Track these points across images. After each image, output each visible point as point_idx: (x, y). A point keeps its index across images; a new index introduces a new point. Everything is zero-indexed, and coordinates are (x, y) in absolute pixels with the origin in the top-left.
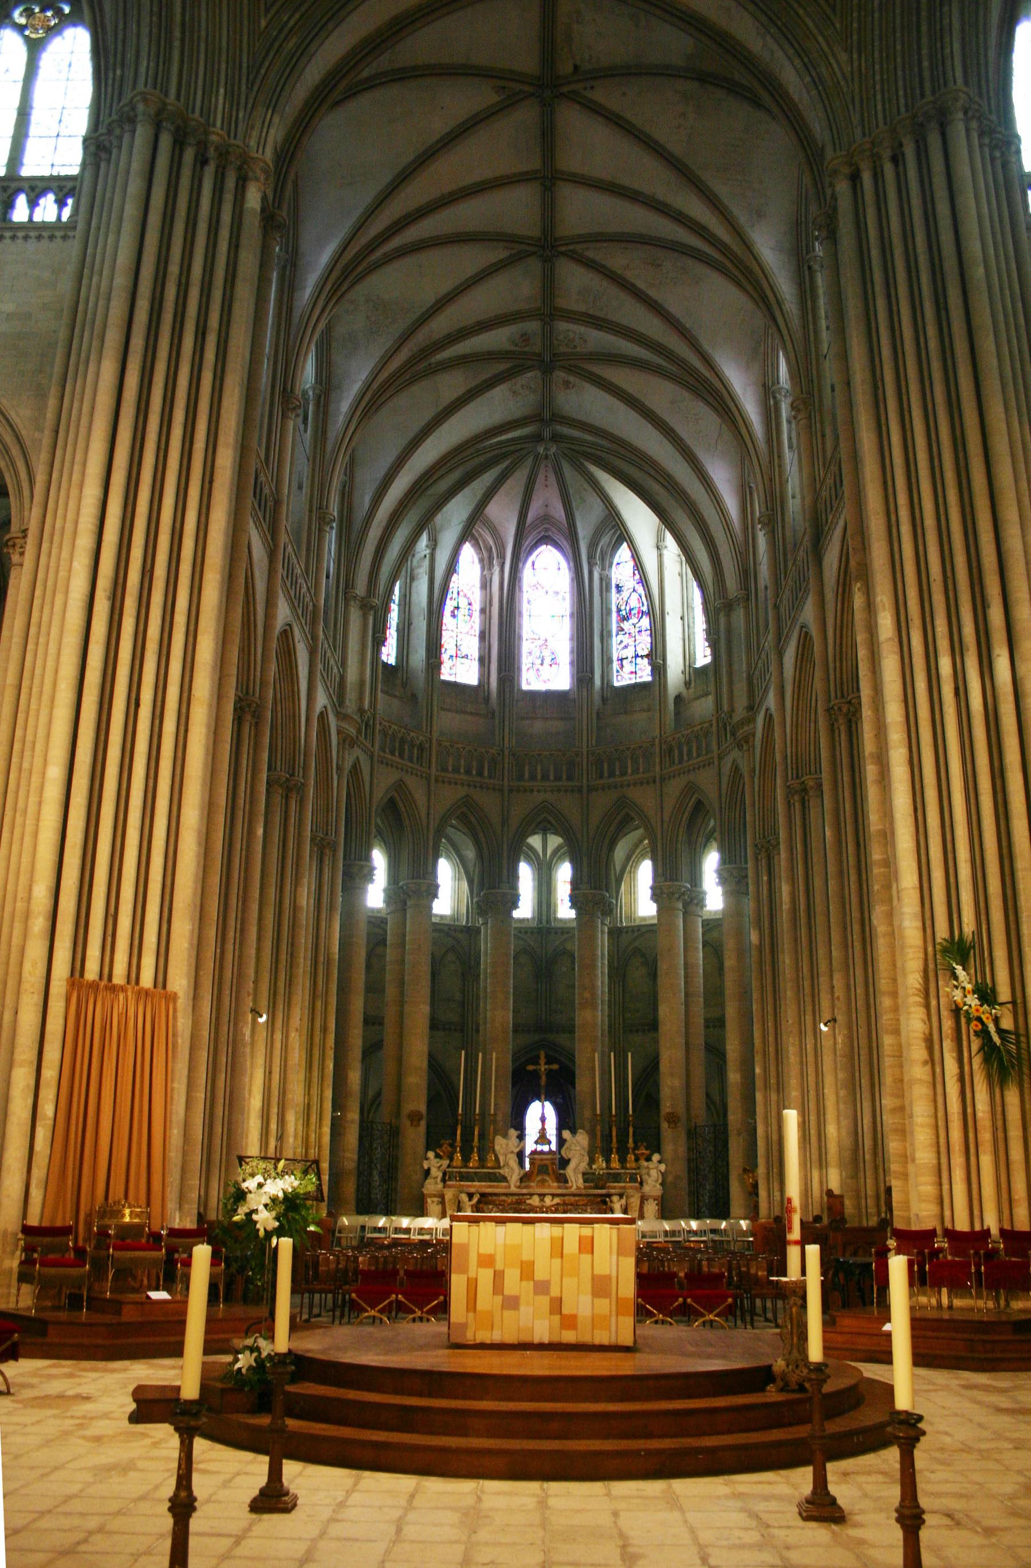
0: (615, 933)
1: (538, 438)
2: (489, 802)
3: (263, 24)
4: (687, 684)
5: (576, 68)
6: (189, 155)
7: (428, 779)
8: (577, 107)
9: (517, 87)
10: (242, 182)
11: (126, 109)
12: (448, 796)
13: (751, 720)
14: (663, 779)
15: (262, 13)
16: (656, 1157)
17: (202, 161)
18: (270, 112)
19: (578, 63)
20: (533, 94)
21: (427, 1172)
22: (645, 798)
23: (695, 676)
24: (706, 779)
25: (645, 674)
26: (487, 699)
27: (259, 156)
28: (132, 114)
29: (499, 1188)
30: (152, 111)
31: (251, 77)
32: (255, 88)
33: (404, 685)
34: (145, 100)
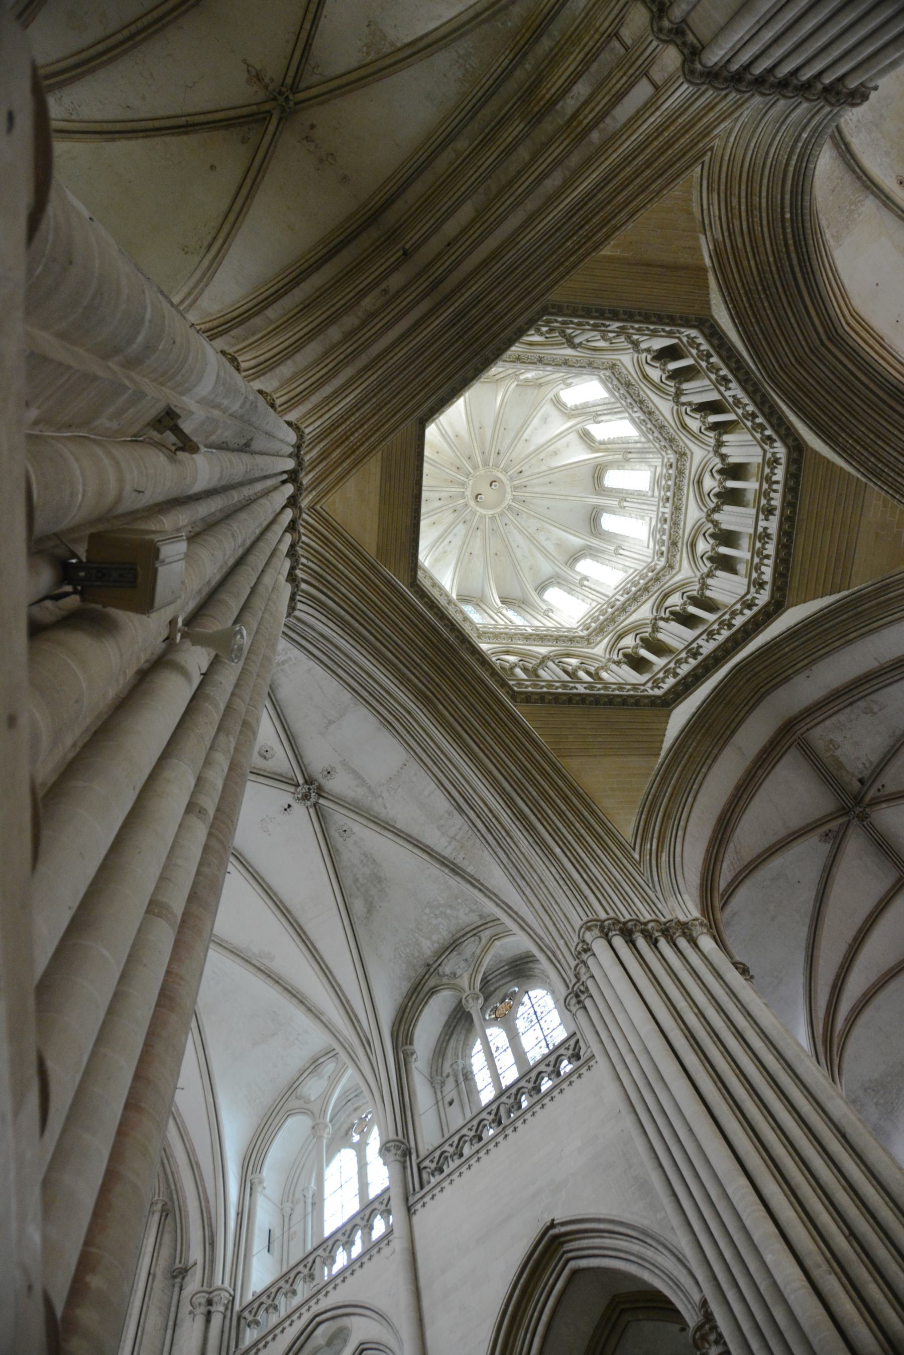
3: (637, 856)
5: (861, 781)
6: (641, 942)
8: (884, 805)
9: (834, 825)
11: (580, 945)
15: (632, 851)
17: (654, 943)
18: (678, 896)
19: (860, 776)
20: (849, 821)
27: (690, 918)
28: (585, 947)
30: (596, 932)
31: (651, 885)
32: (658, 888)
34: (589, 929)
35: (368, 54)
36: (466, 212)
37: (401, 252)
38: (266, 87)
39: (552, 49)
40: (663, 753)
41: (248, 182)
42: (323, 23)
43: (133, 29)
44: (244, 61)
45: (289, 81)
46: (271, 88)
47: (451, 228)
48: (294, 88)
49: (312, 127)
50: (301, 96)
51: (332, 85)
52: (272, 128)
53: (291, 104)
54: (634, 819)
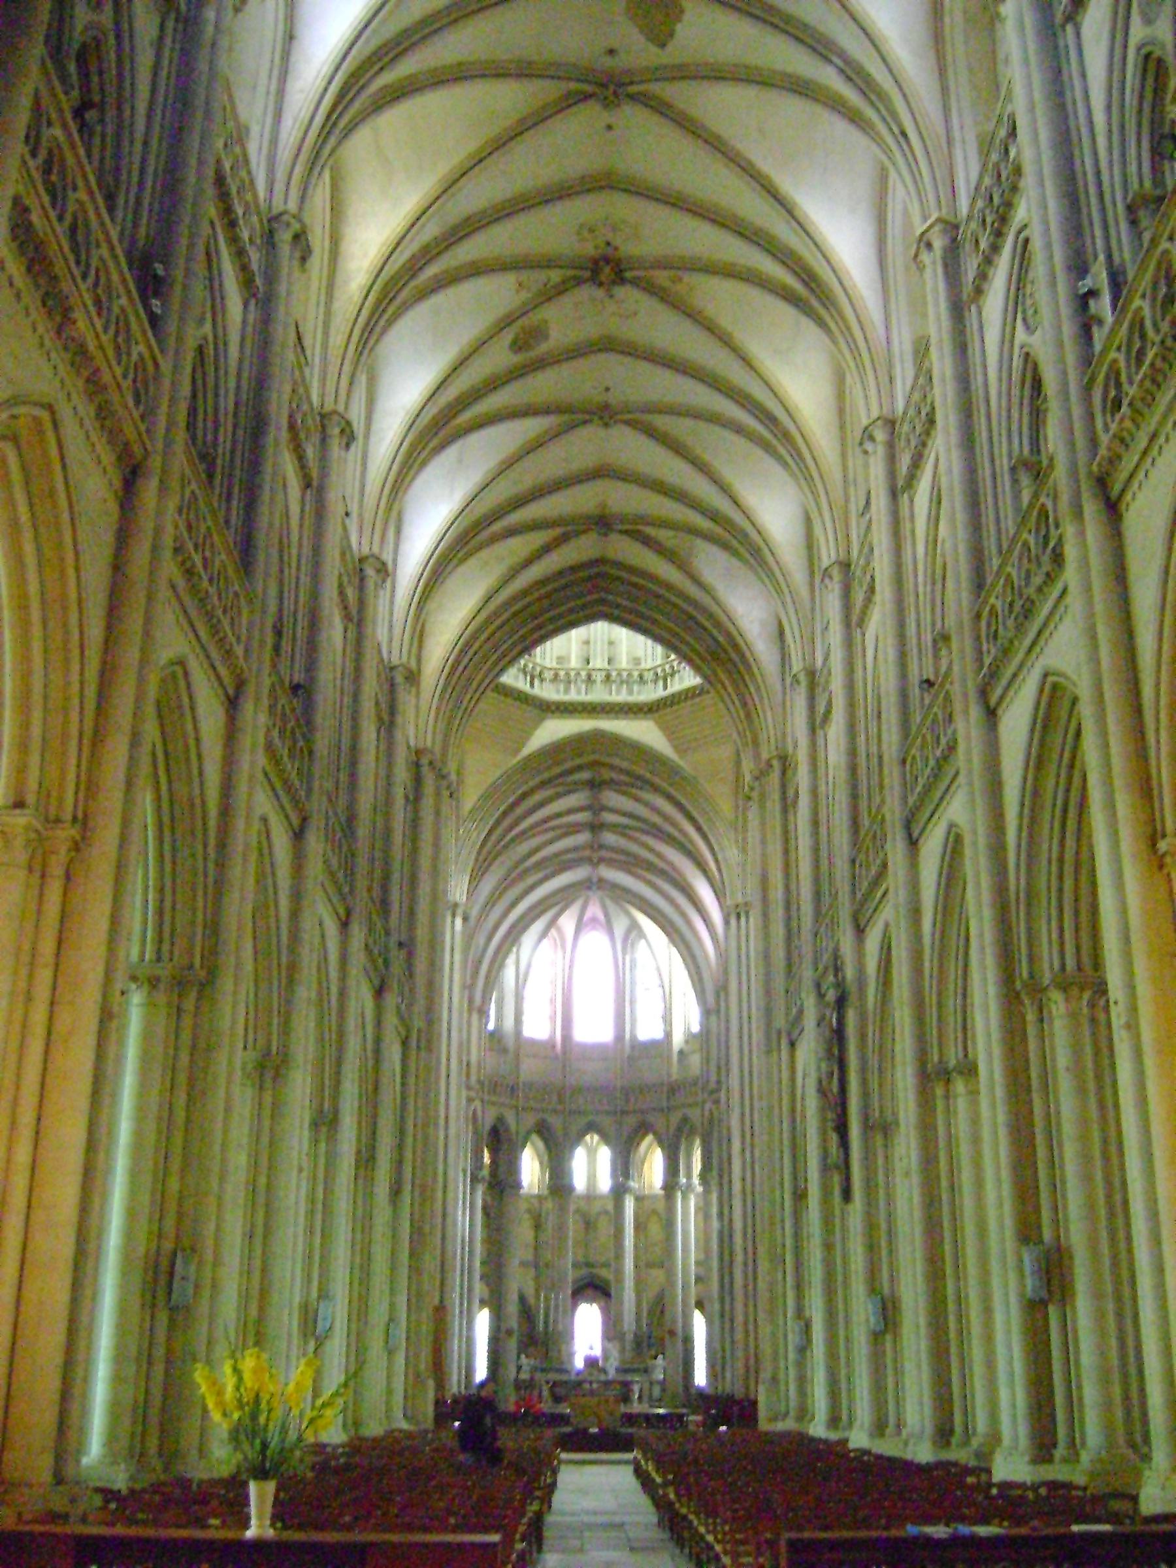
0: (639, 1199)
1: (589, 888)
2: (555, 1122)
4: (687, 1042)
7: (516, 1108)
10: (454, 916)
12: (530, 1120)
13: (718, 1090)
14: (669, 1109)
16: (660, 1357)
21: (519, 1368)
22: (659, 1121)
23: (690, 1038)
24: (694, 1114)
25: (658, 1034)
26: (554, 1046)
29: (564, 1377)
33: (499, 1041)
40: (519, 758)
54: (475, 798)
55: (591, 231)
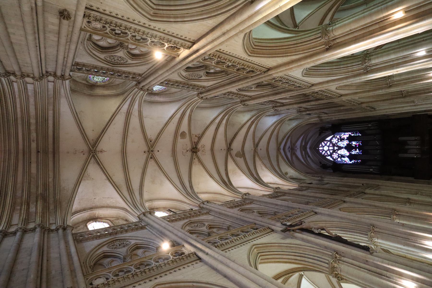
35: (87, 174)
36: (34, 170)
37: (39, 151)
38: (98, 152)
39: (49, 208)
41: (83, 133)
42: (100, 170)
43: (126, 136)
44: (106, 151)
45: (95, 156)
46: (98, 152)
47: (34, 166)
48: (93, 156)
49: (84, 154)
50: (91, 156)
51: (87, 163)
52: (90, 145)
53: (91, 153)
55: (203, 147)
